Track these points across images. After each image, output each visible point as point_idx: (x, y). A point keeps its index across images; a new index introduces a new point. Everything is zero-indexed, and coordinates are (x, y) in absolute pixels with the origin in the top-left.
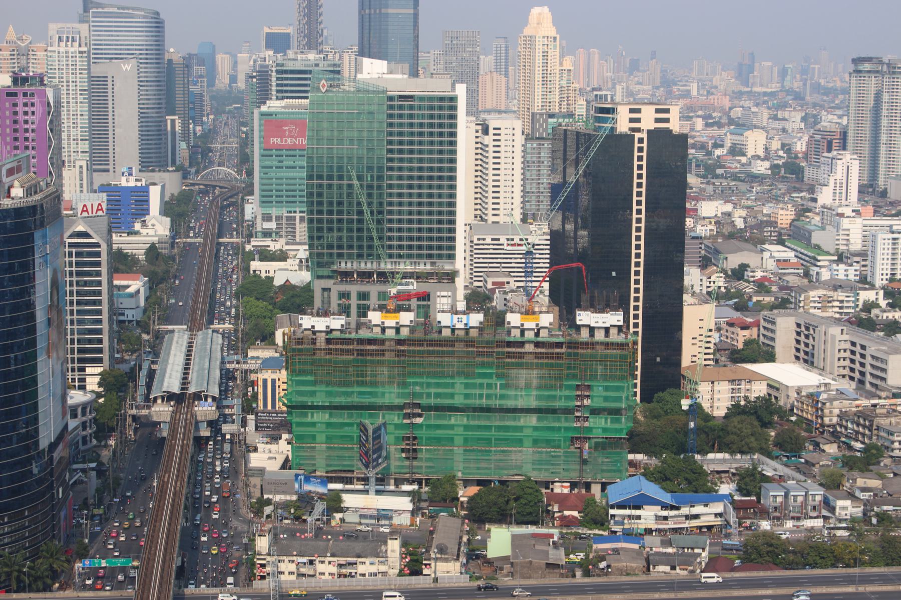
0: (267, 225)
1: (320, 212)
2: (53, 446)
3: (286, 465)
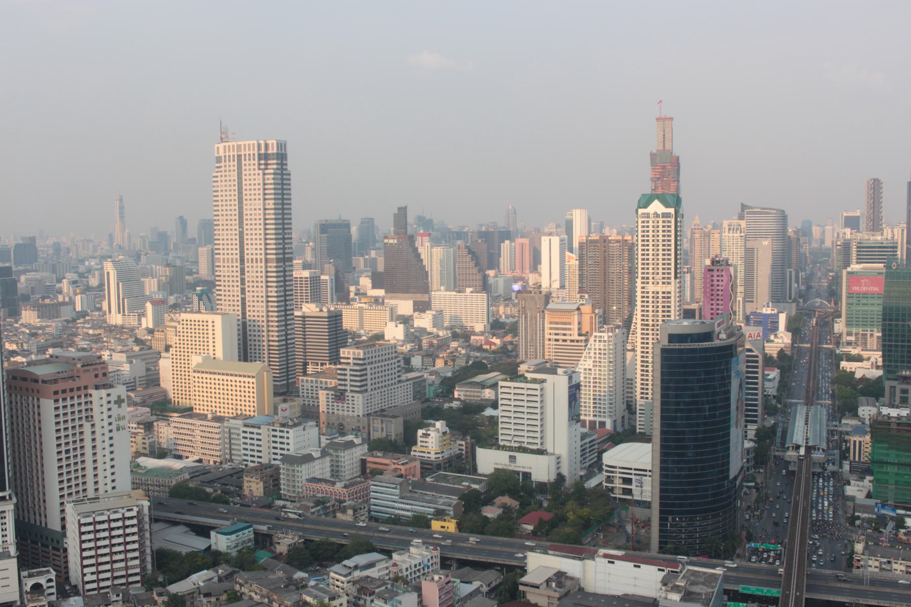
0: (849, 338)
1: (890, 341)
2: (736, 478)
3: (869, 496)
